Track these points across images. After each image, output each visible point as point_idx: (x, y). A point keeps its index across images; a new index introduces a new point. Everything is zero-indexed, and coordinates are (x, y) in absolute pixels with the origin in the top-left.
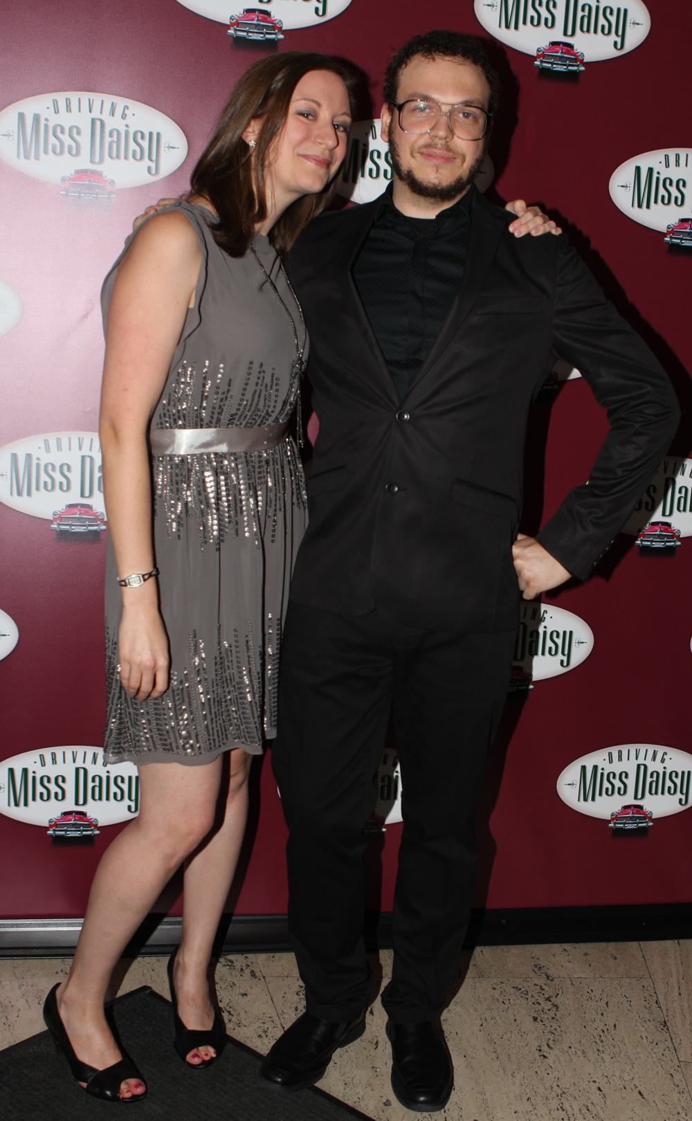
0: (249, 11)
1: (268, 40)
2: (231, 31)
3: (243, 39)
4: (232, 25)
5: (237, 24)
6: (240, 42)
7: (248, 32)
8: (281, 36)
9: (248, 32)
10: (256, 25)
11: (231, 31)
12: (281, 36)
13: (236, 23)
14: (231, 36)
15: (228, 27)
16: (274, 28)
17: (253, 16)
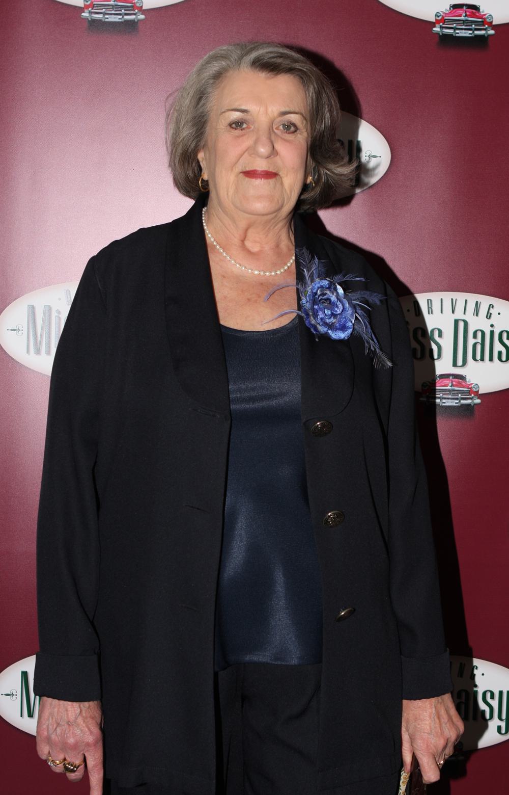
0: (455, 7)
1: (477, 36)
2: (437, 29)
3: (451, 36)
4: (438, 22)
5: (443, 20)
6: (446, 40)
7: (455, 29)
8: (492, 32)
9: (455, 29)
10: (464, 21)
11: (437, 29)
12: (492, 32)
13: (442, 20)
14: (437, 34)
15: (433, 24)
16: (484, 23)
17: (460, 11)
